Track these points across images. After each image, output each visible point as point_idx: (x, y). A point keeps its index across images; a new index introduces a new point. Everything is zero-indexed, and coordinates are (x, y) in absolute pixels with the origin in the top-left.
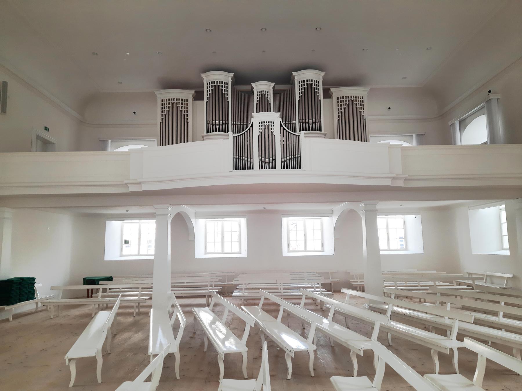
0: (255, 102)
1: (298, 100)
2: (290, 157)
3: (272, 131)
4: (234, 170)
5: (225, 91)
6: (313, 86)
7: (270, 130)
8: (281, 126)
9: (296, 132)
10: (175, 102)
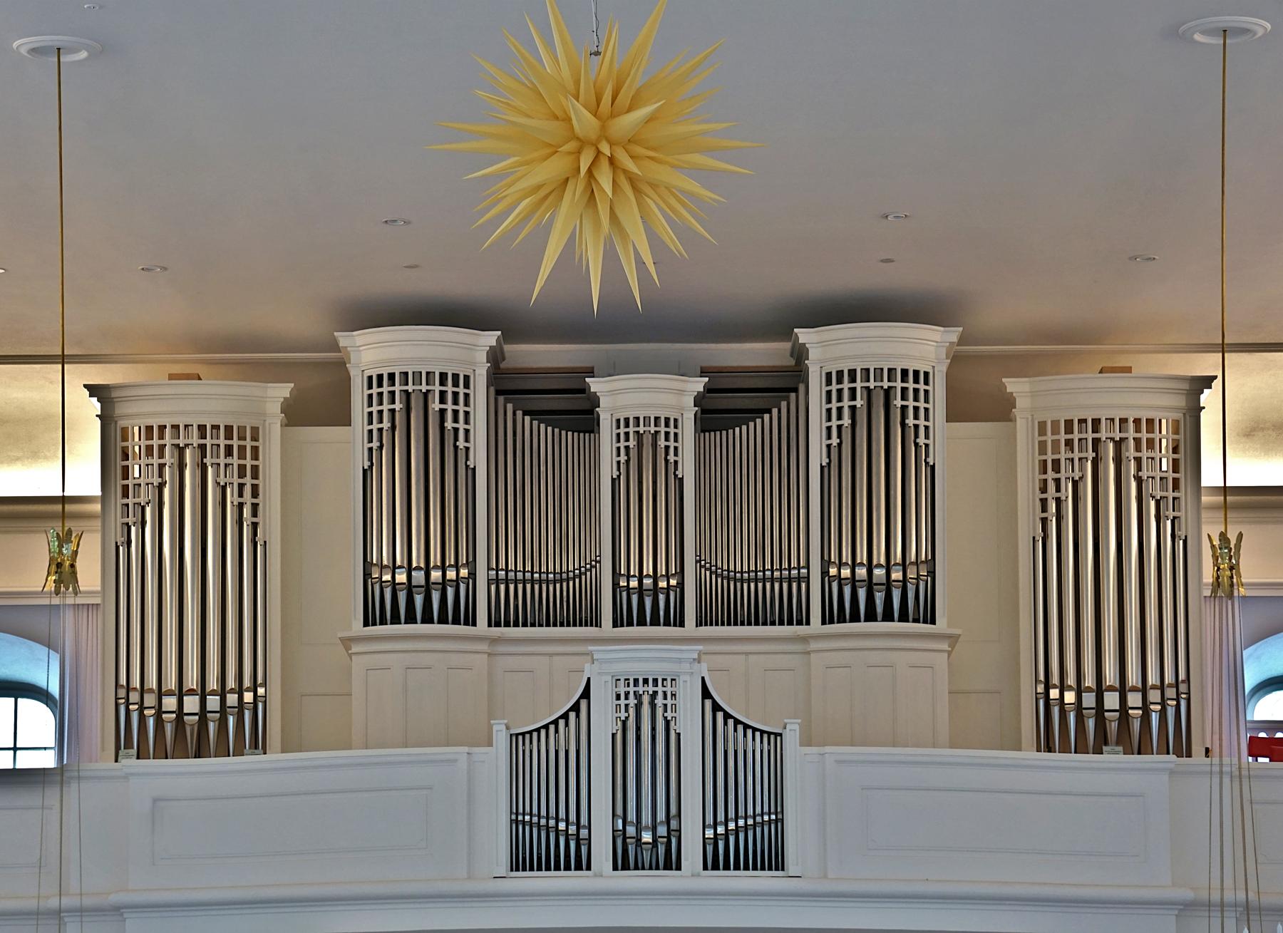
0: (607, 471)
1: (822, 467)
2: (741, 822)
3: (669, 718)
4: (512, 870)
5: (456, 420)
6: (898, 402)
7: (660, 711)
8: (703, 698)
9: (808, 623)
10: (196, 441)
